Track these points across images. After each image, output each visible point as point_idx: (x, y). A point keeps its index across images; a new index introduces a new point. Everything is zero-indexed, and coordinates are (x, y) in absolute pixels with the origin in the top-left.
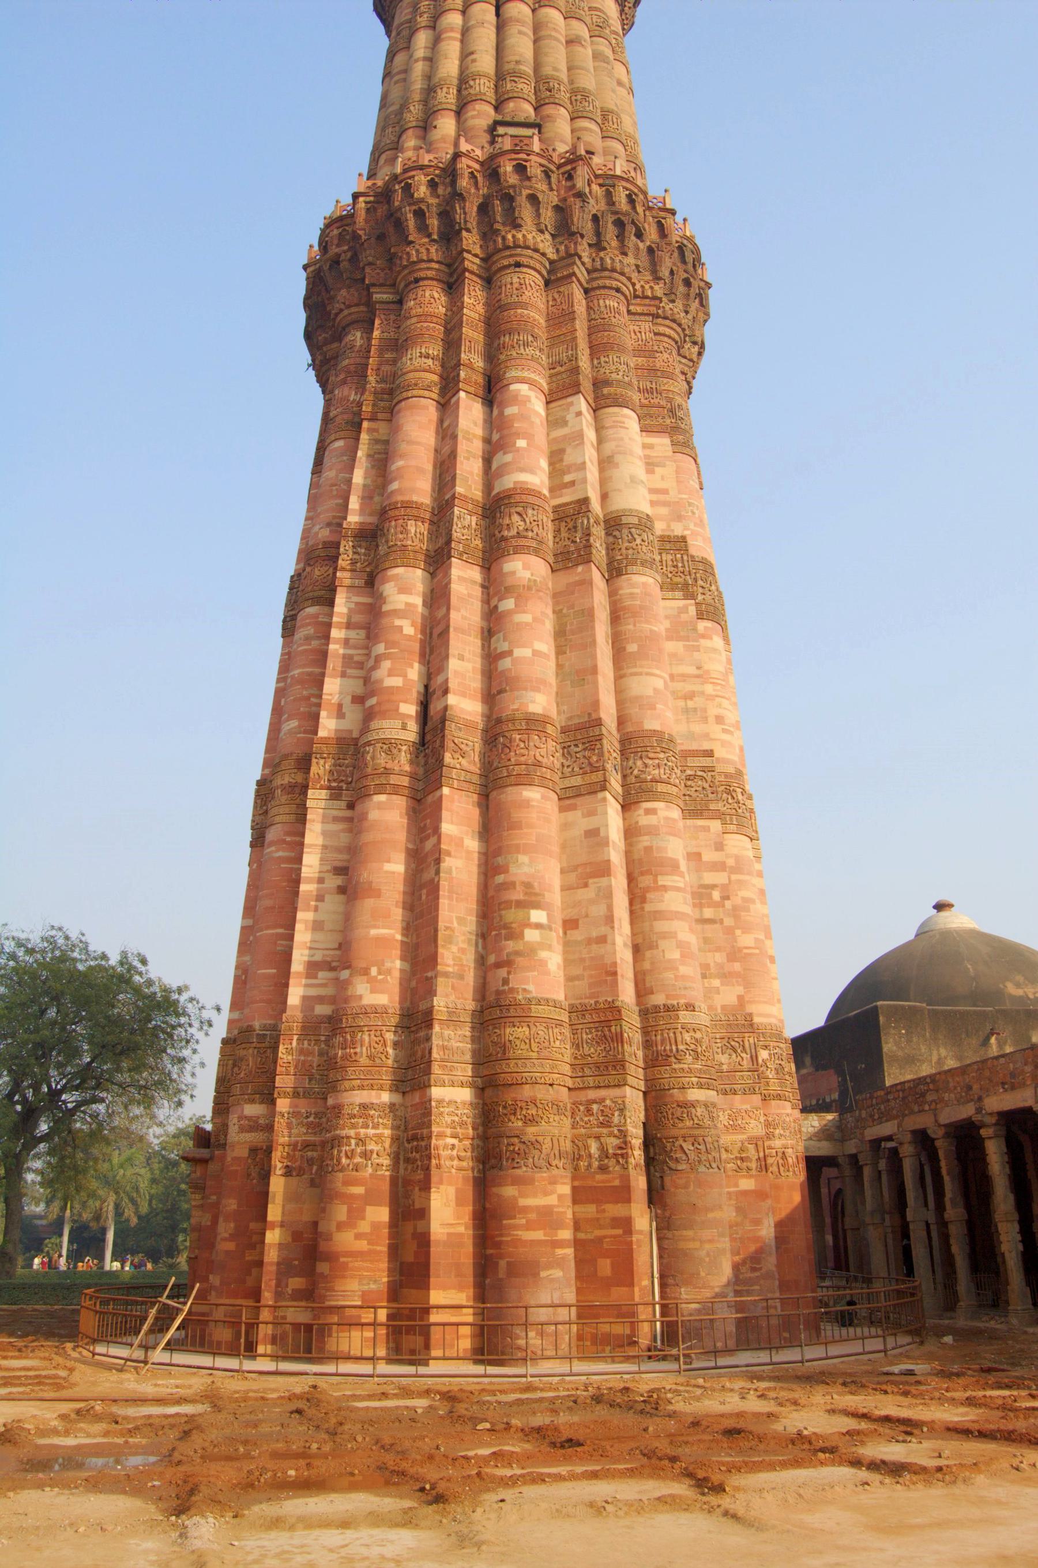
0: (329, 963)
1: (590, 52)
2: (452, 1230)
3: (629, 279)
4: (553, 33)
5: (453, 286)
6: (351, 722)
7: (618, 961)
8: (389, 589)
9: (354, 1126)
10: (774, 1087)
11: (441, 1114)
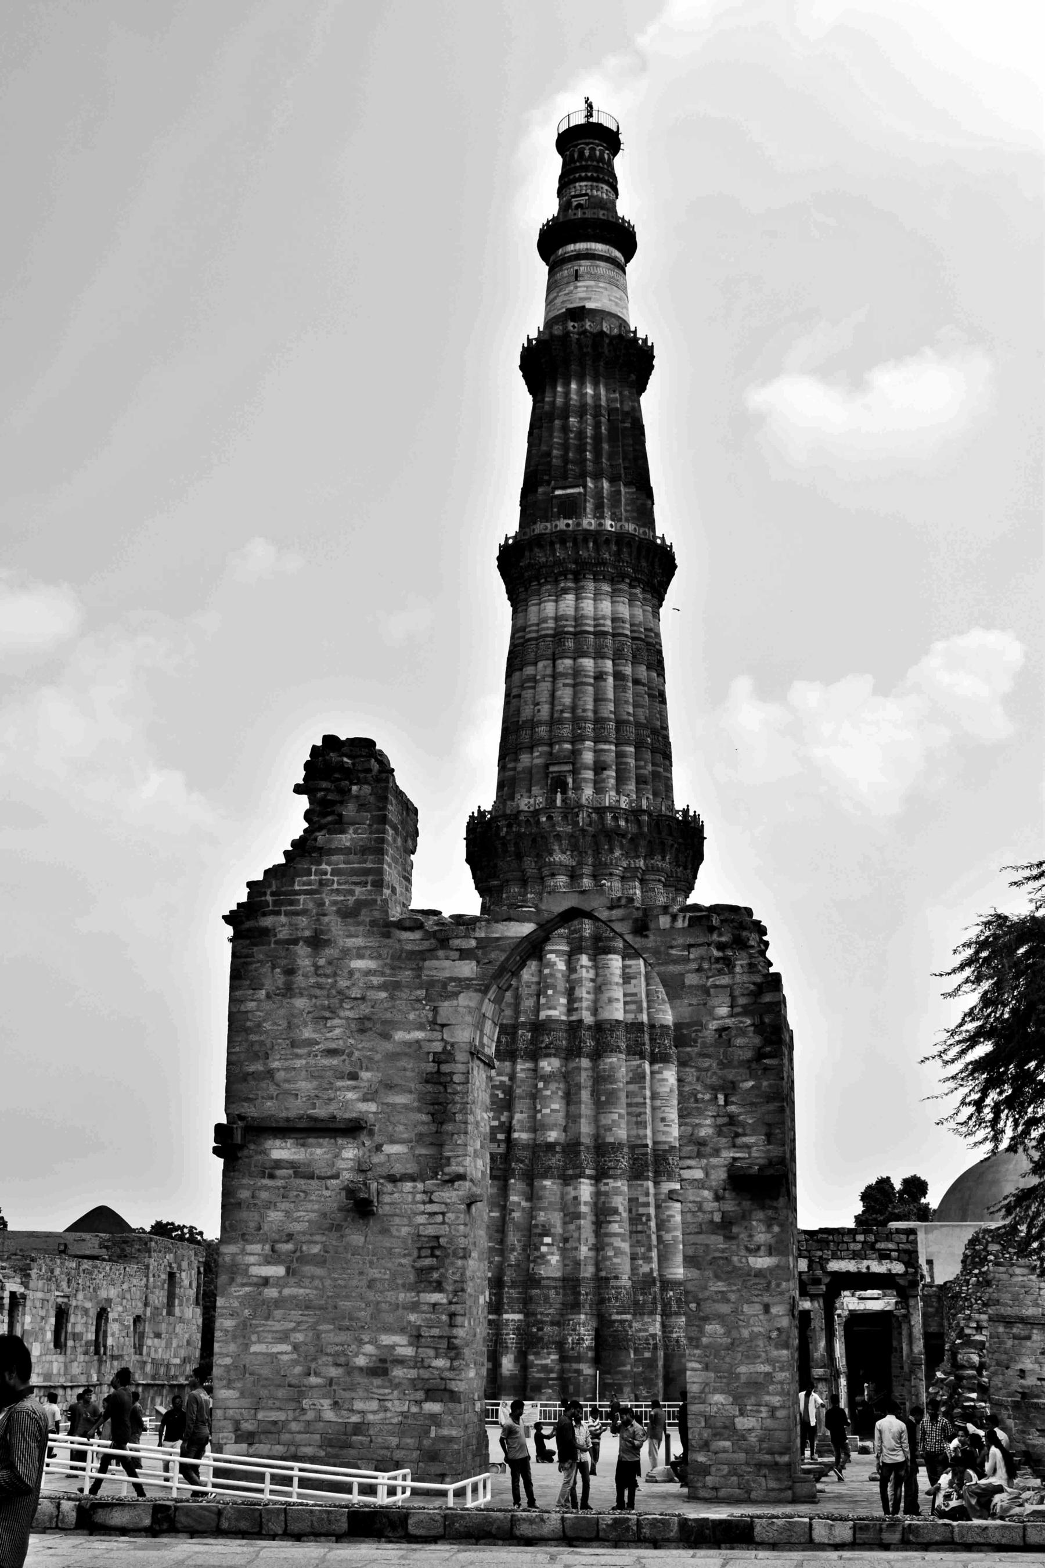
1: (610, 680)
5: (524, 882)
7: (582, 1258)
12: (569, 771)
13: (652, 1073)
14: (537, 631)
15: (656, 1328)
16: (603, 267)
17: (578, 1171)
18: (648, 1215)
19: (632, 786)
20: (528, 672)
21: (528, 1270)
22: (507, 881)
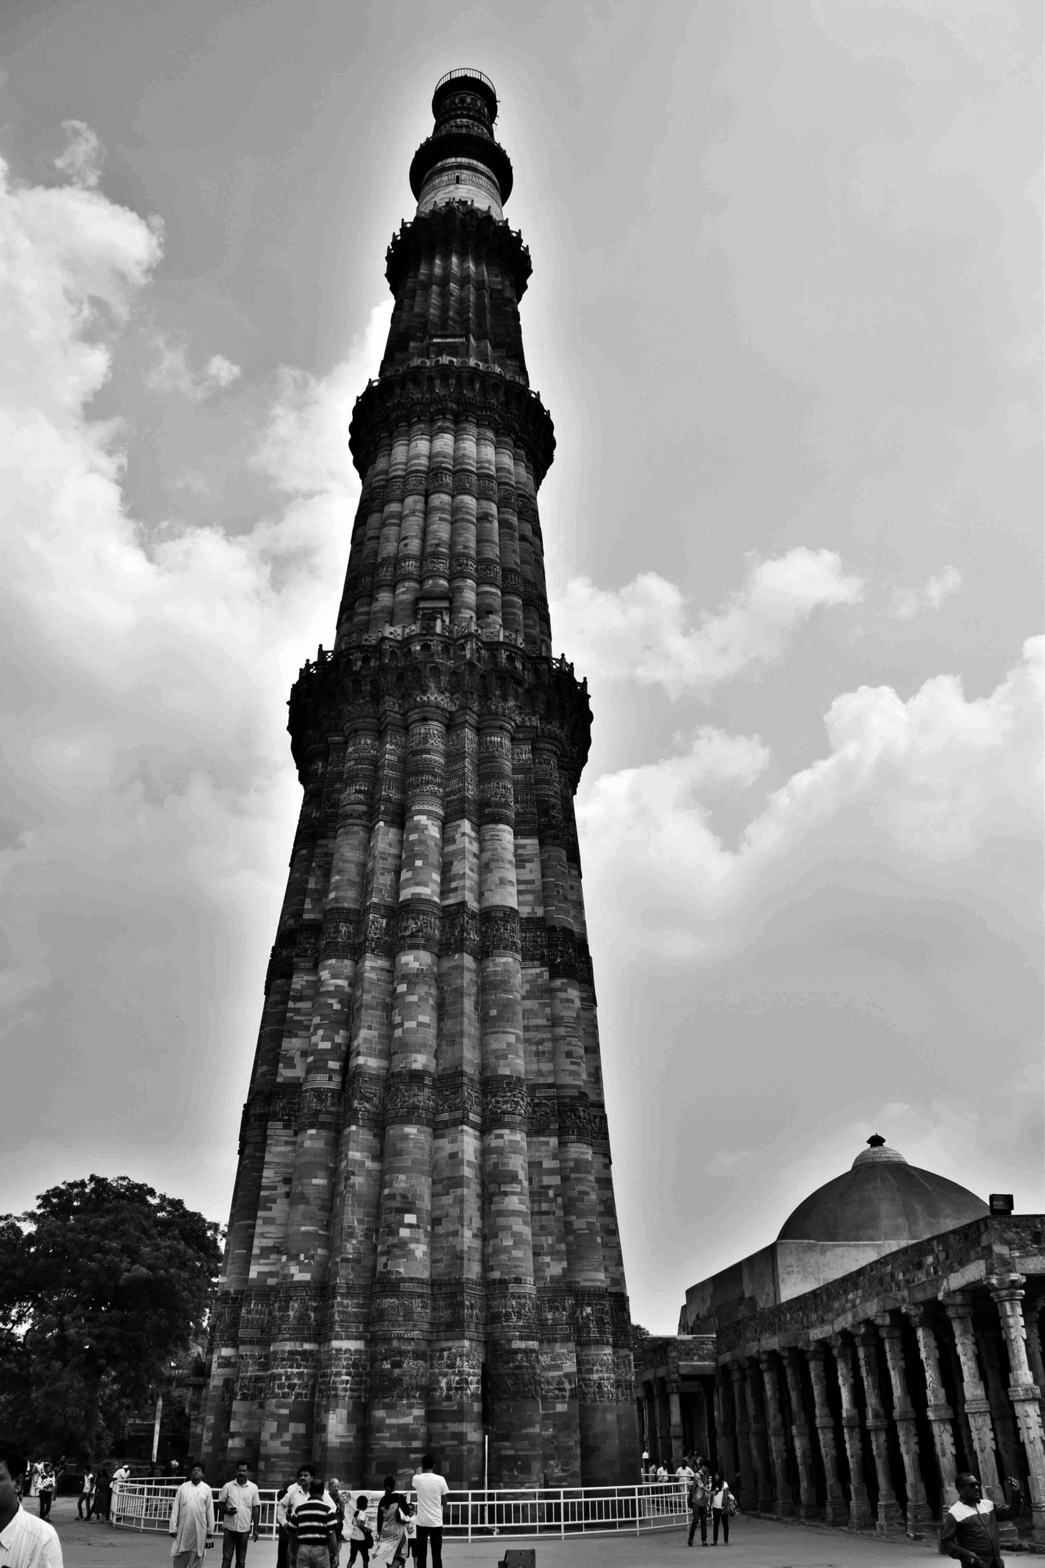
0: (278, 1248)
1: (496, 524)
2: (344, 1440)
3: (511, 718)
4: (466, 517)
6: (298, 1072)
7: (466, 1249)
8: (325, 974)
9: (284, 1367)
10: (594, 1334)
11: (339, 1359)
12: (446, 608)
14: (405, 470)
16: (484, 181)
17: (458, 1114)
20: (392, 509)
21: (375, 1266)
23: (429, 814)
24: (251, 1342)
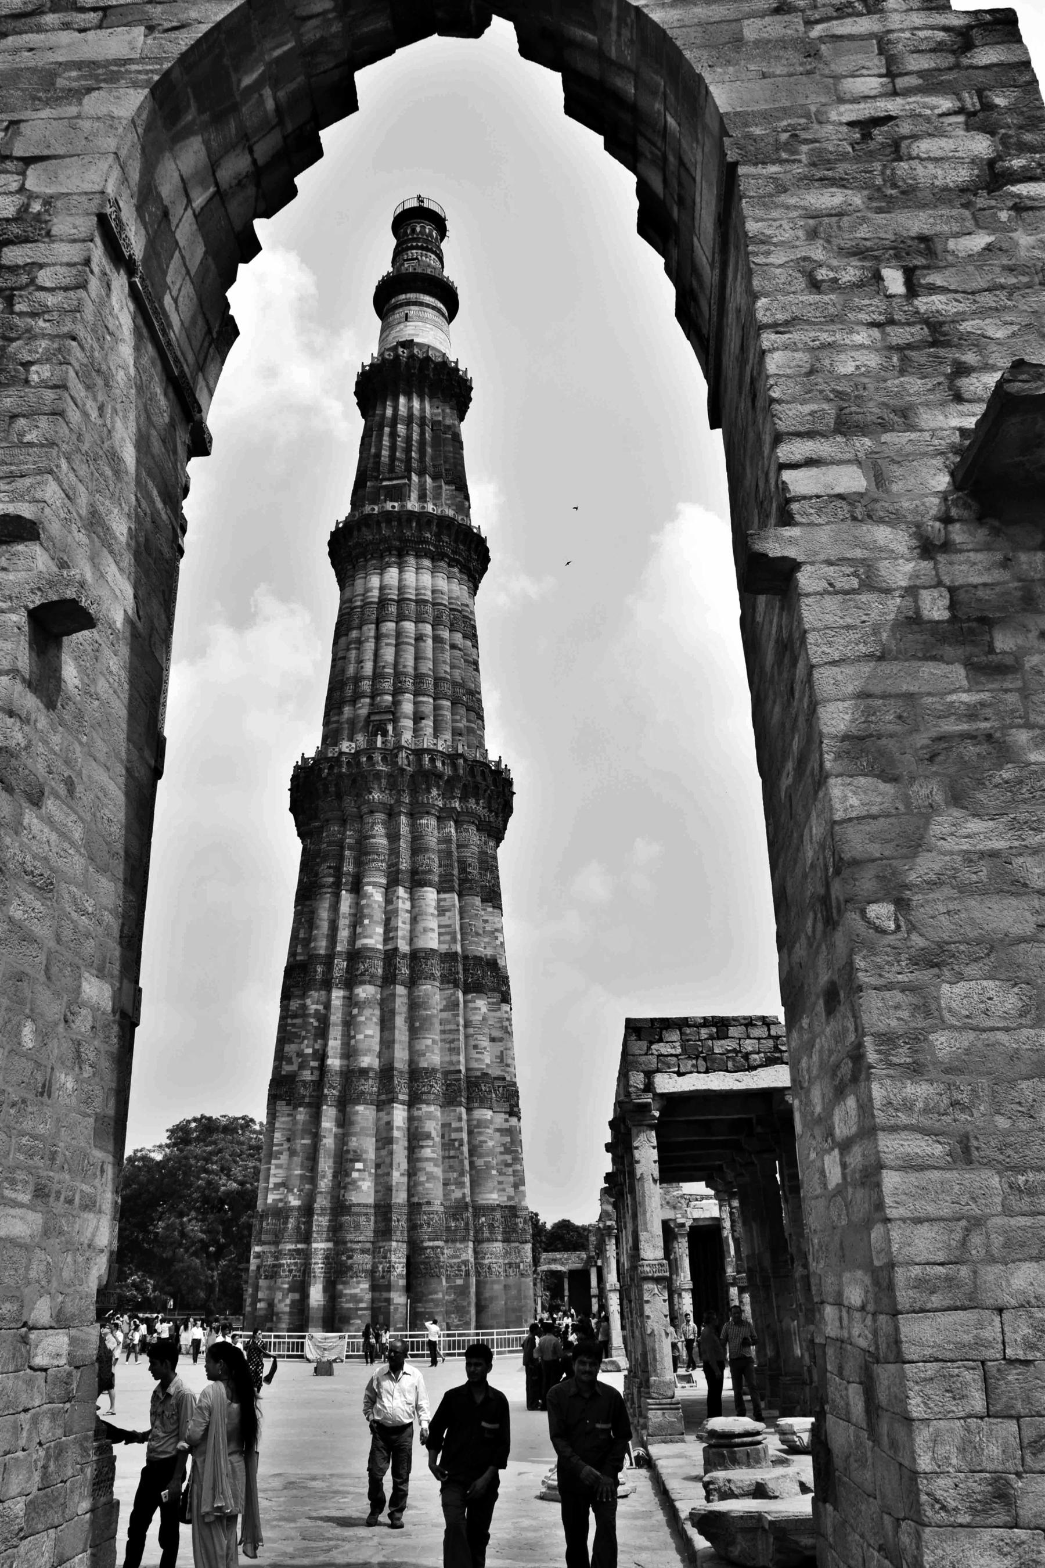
1: (430, 641)
6: (294, 1067)
8: (308, 1001)
10: (486, 1234)
13: (465, 1002)
15: (469, 1255)
16: (430, 314)
17: (390, 1096)
18: (461, 1141)
19: (448, 736)
22: (327, 821)
23: (375, 885)
24: (269, 1243)
